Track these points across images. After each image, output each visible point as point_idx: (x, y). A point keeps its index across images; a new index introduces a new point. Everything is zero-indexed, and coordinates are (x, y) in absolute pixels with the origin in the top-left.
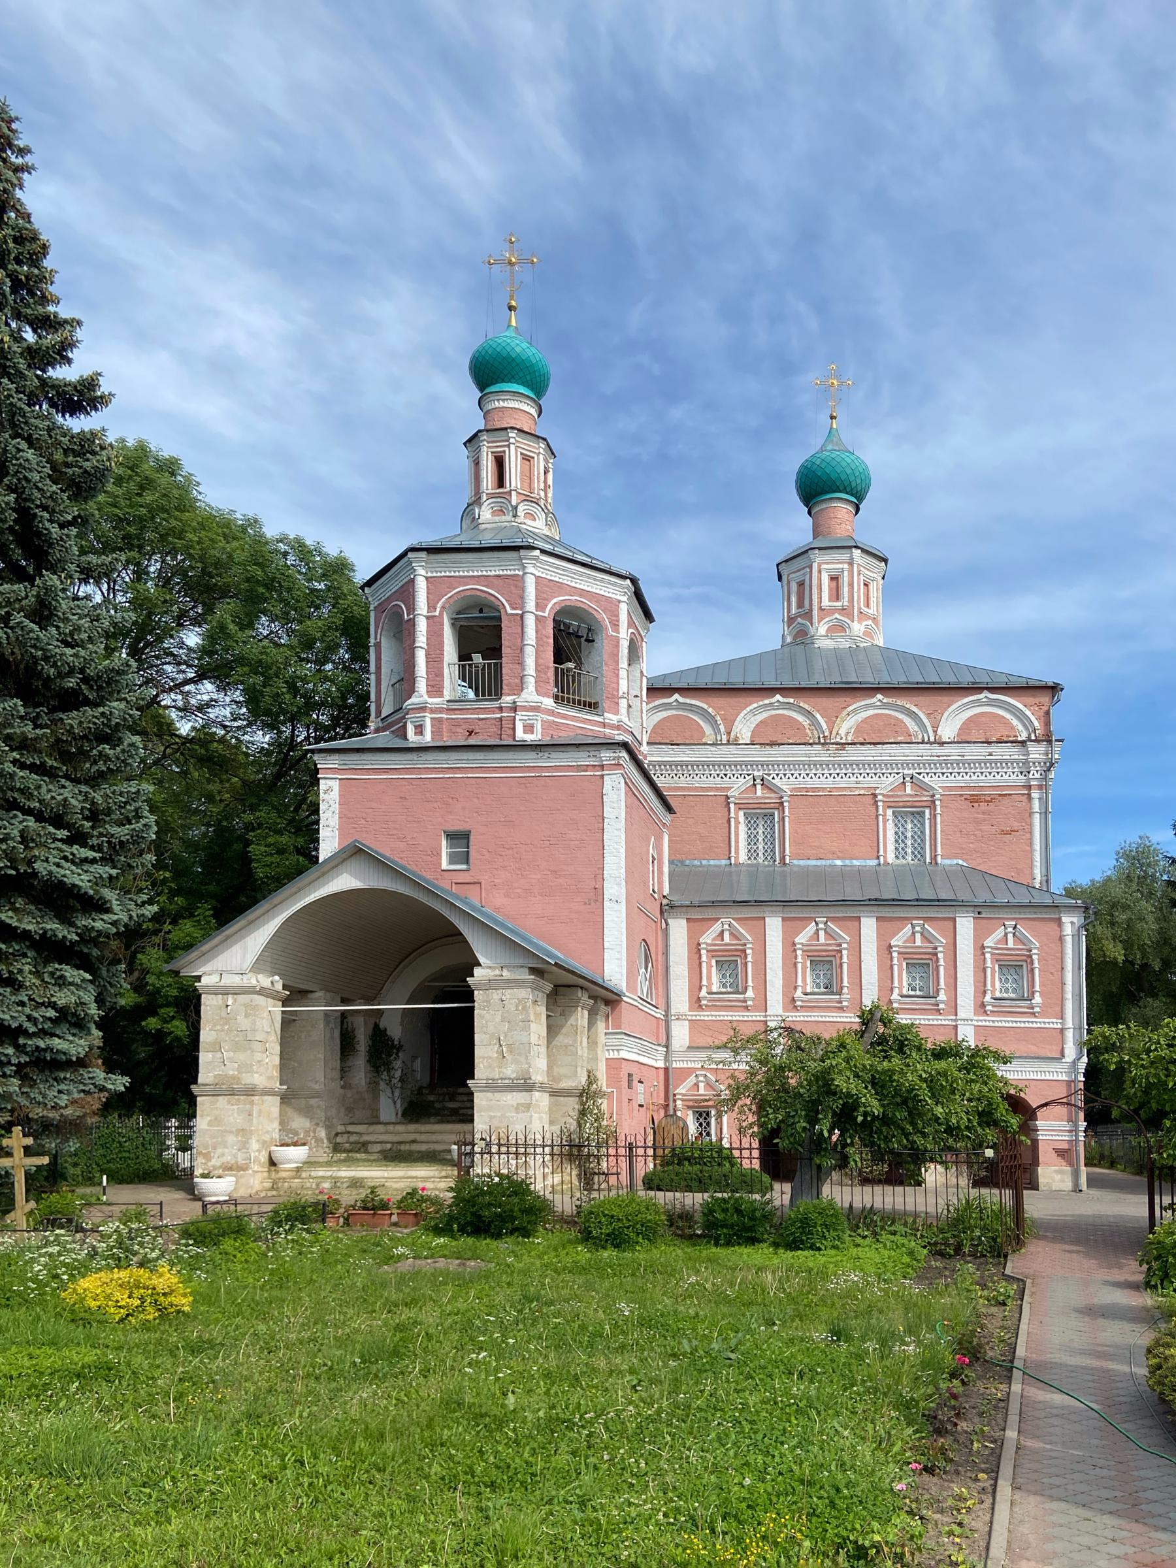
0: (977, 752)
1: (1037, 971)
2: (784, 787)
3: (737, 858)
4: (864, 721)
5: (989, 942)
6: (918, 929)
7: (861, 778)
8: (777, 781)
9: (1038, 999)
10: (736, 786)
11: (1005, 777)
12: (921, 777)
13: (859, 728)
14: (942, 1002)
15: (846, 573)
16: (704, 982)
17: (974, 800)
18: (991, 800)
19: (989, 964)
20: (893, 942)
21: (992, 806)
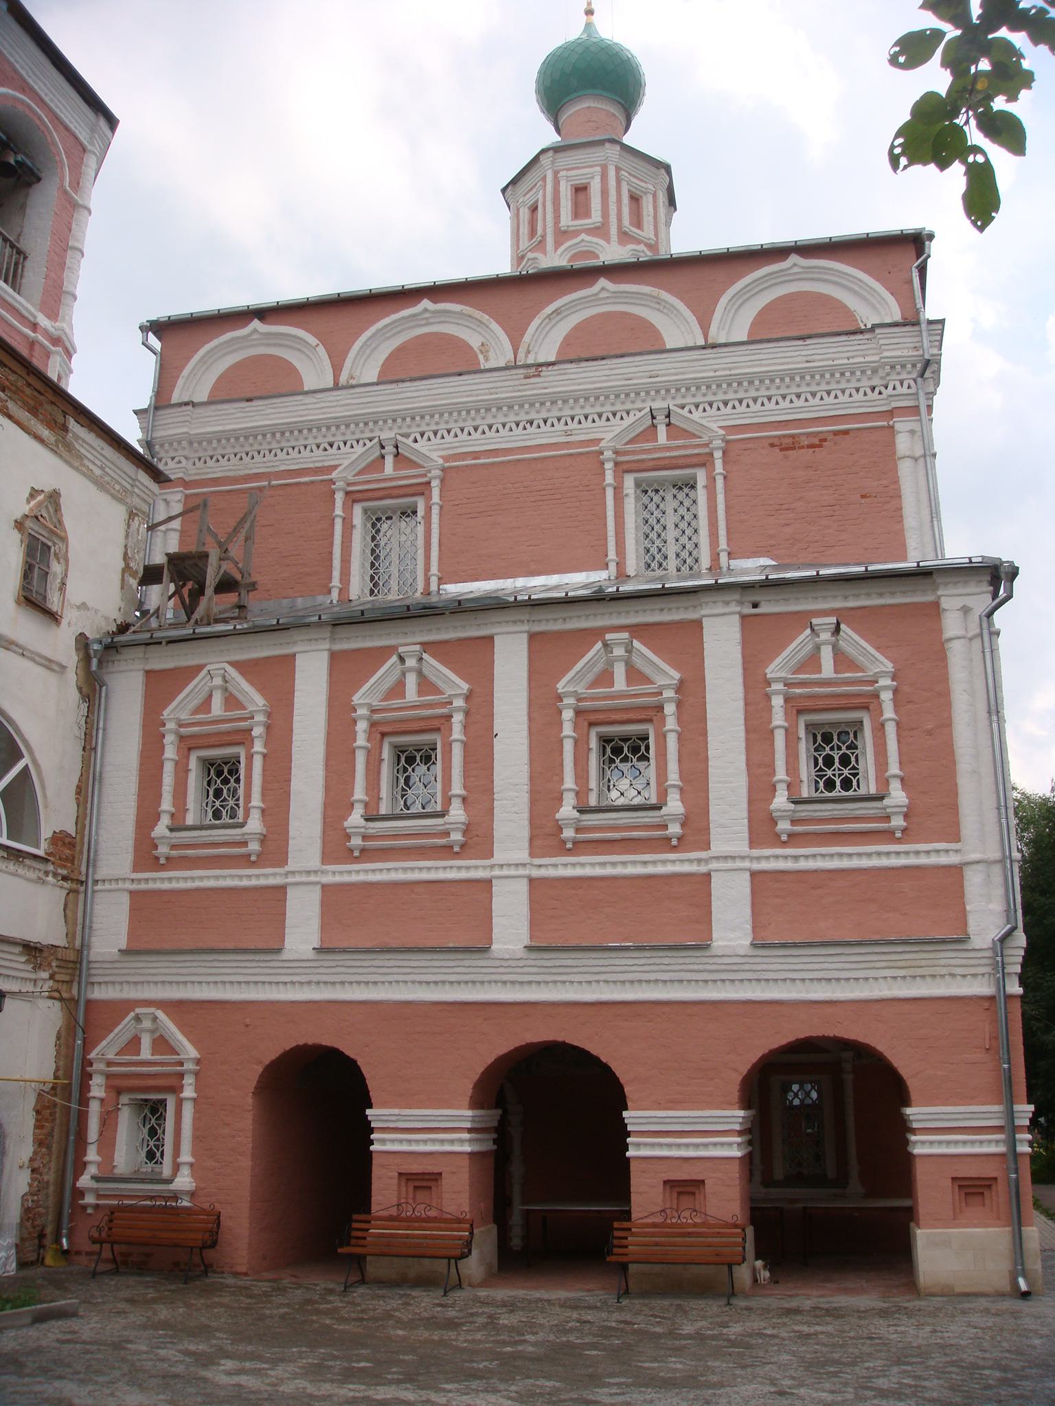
0: (789, 356)
1: (891, 729)
2: (434, 455)
3: (344, 590)
4: (578, 328)
5: (777, 669)
6: (619, 651)
7: (573, 425)
8: (422, 446)
9: (897, 796)
10: (346, 463)
11: (842, 398)
12: (685, 412)
13: (567, 342)
14: (674, 818)
15: (598, 179)
16: (166, 804)
17: (788, 446)
18: (819, 443)
19: (779, 719)
20: (561, 686)
21: (821, 454)
